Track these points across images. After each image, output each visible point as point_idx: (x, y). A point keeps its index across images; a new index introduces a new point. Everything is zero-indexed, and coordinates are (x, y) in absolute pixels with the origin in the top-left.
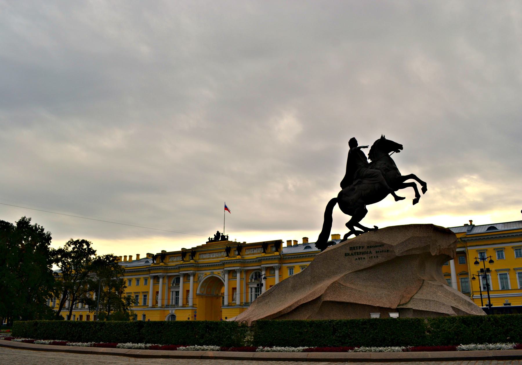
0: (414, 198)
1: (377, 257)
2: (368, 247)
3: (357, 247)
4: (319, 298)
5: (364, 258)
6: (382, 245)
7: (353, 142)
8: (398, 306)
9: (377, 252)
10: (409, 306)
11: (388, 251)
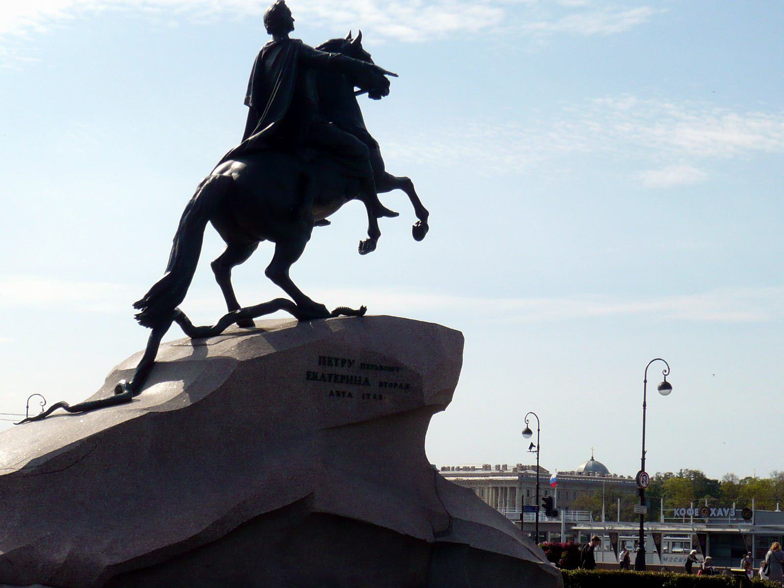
0: (365, 237)
1: (381, 397)
2: (363, 366)
3: (337, 360)
4: (300, 504)
5: (350, 395)
6: (396, 368)
7: (279, 20)
8: (436, 535)
9: (381, 384)
10: (458, 537)
11: (407, 387)
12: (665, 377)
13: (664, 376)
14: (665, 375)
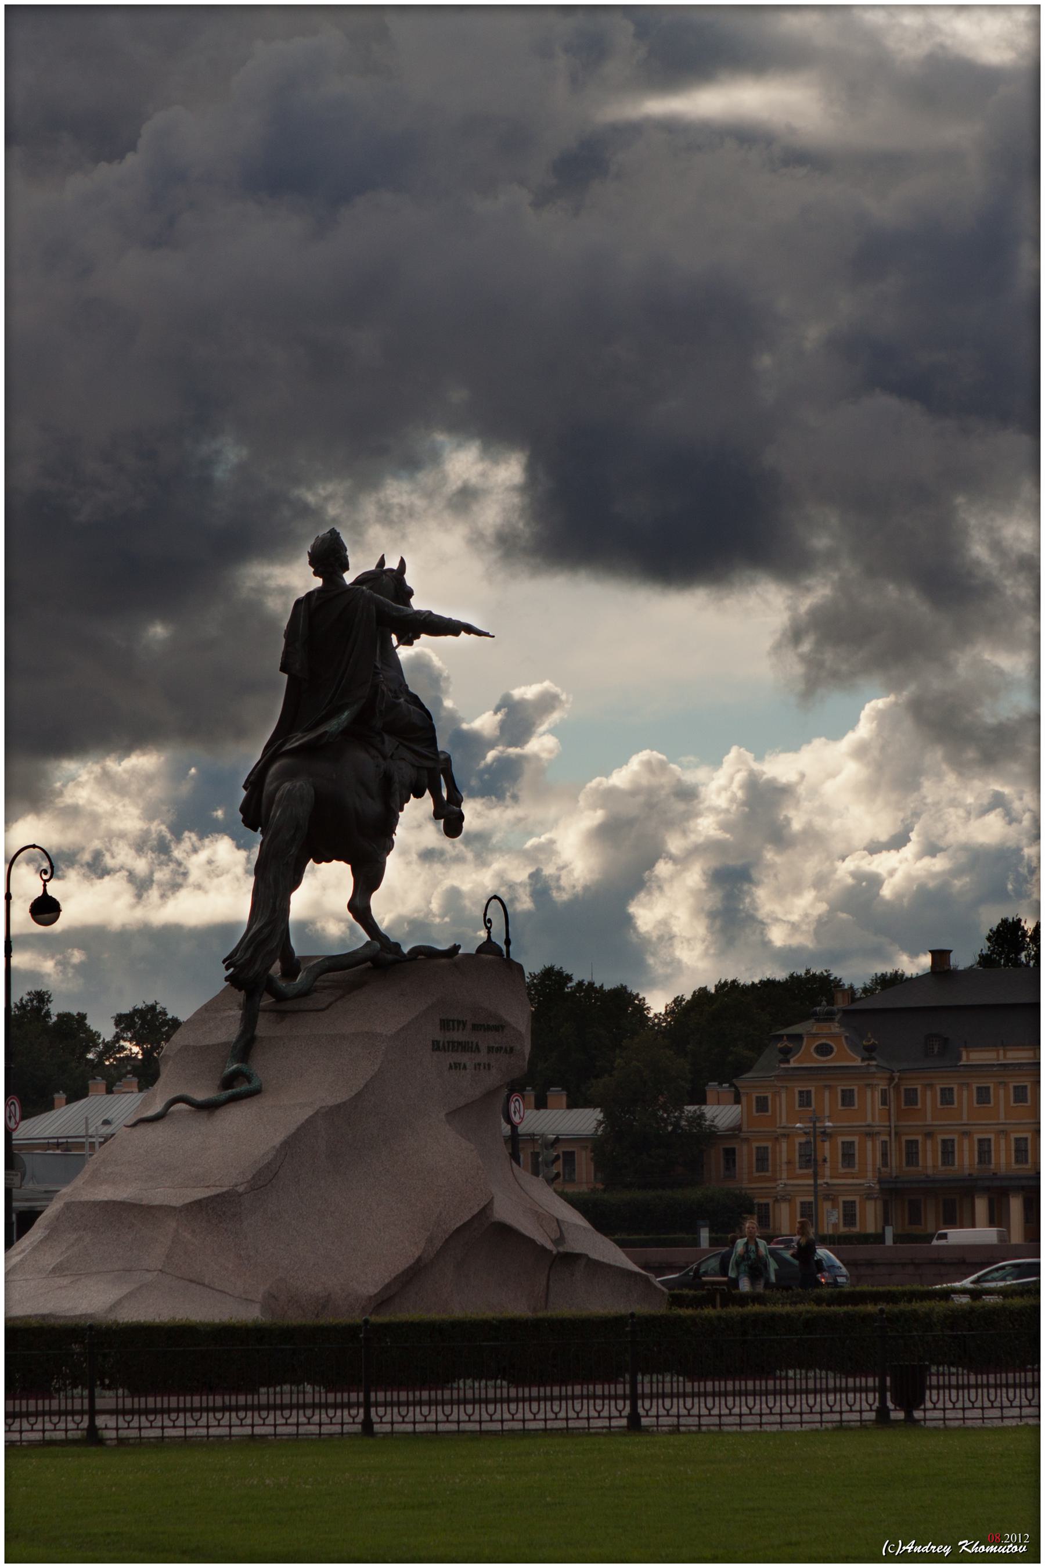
9: (490, 1050)
12: (45, 886)
13: (42, 883)
14: (45, 881)
